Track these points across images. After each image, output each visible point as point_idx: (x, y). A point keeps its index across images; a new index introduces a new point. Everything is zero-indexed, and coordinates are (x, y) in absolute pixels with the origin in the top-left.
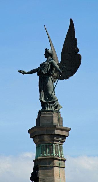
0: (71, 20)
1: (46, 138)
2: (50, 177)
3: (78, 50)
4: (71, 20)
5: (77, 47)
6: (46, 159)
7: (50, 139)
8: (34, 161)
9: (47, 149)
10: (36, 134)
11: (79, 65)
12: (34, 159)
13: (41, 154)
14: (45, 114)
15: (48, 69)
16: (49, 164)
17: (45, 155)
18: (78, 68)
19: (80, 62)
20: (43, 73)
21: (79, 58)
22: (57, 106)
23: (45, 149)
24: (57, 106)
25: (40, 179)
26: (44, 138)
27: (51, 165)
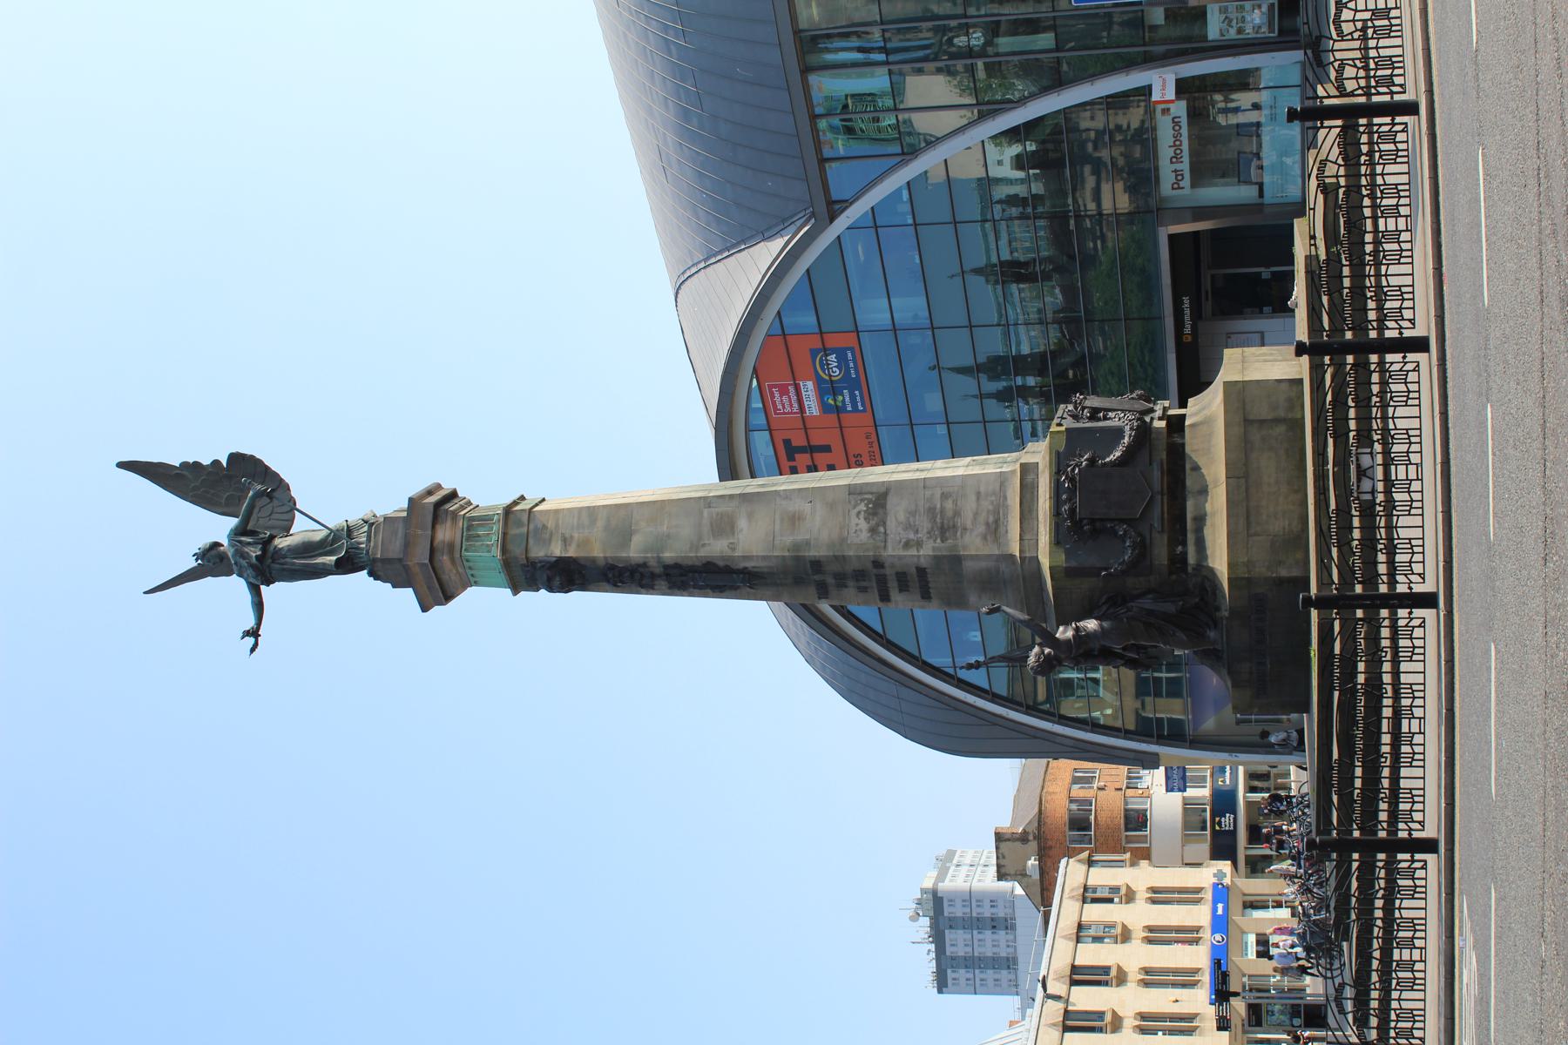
0: (123, 465)
1: (444, 534)
2: (560, 522)
3: (216, 463)
4: (121, 465)
5: (207, 465)
6: (505, 534)
7: (449, 523)
8: (516, 591)
9: (479, 536)
10: (427, 561)
11: (260, 462)
12: (508, 591)
13: (489, 551)
14: (376, 546)
15: (249, 544)
16: (519, 524)
17: (494, 538)
18: (267, 468)
19: (252, 457)
20: (256, 556)
21: (236, 458)
22: (363, 520)
23: (477, 541)
24: (363, 520)
25: (561, 553)
26: (444, 542)
27: (525, 518)
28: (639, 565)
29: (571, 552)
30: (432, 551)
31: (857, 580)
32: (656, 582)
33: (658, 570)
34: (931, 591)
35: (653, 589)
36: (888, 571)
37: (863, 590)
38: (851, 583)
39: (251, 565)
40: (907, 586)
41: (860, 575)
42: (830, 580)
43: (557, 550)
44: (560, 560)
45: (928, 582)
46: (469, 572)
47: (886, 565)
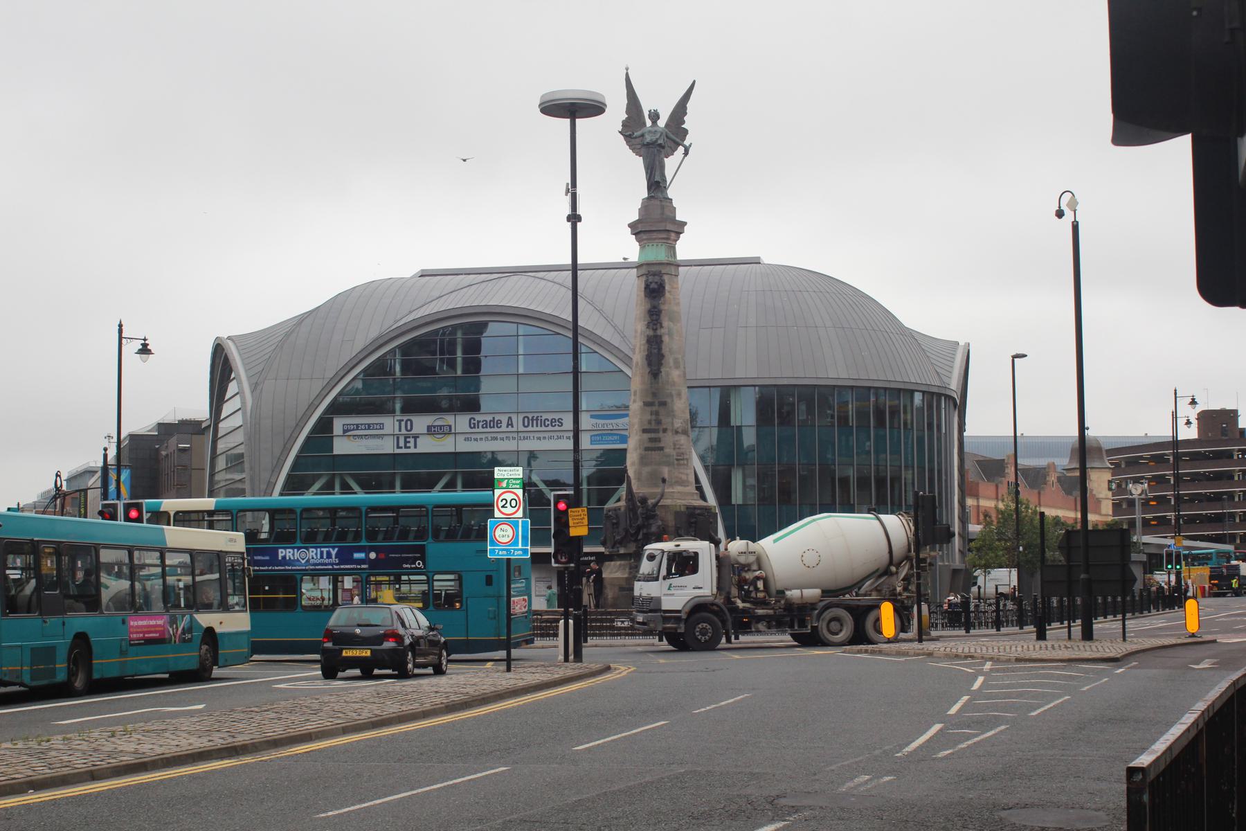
28: (661, 324)
29: (667, 295)
30: (668, 231)
31: (655, 420)
32: (651, 330)
33: (659, 332)
34: (650, 452)
35: (647, 328)
36: (661, 435)
37: (650, 422)
38: (654, 417)
39: (657, 139)
40: (652, 442)
41: (659, 422)
42: (654, 408)
43: (667, 287)
44: (664, 288)
45: (655, 451)
46: (655, 244)
47: (665, 434)
